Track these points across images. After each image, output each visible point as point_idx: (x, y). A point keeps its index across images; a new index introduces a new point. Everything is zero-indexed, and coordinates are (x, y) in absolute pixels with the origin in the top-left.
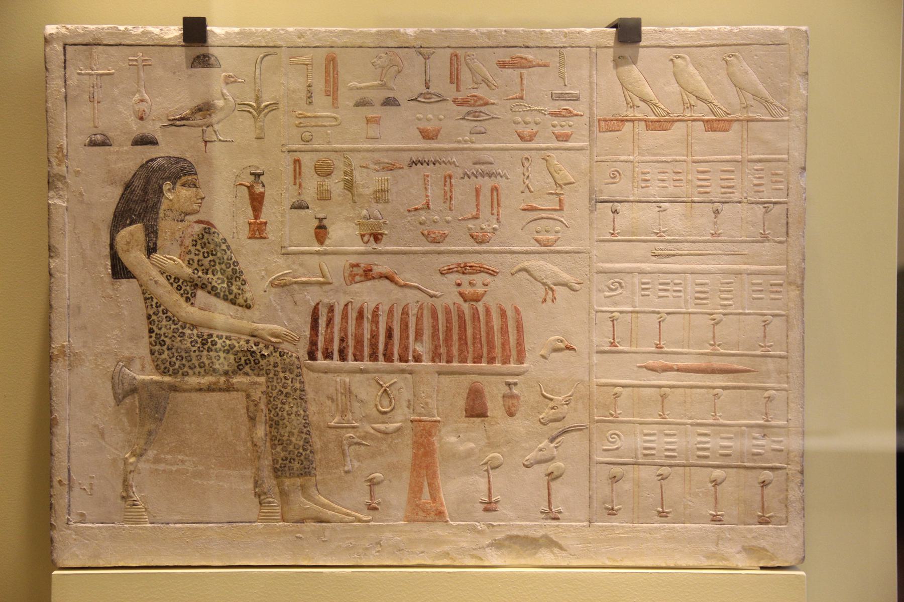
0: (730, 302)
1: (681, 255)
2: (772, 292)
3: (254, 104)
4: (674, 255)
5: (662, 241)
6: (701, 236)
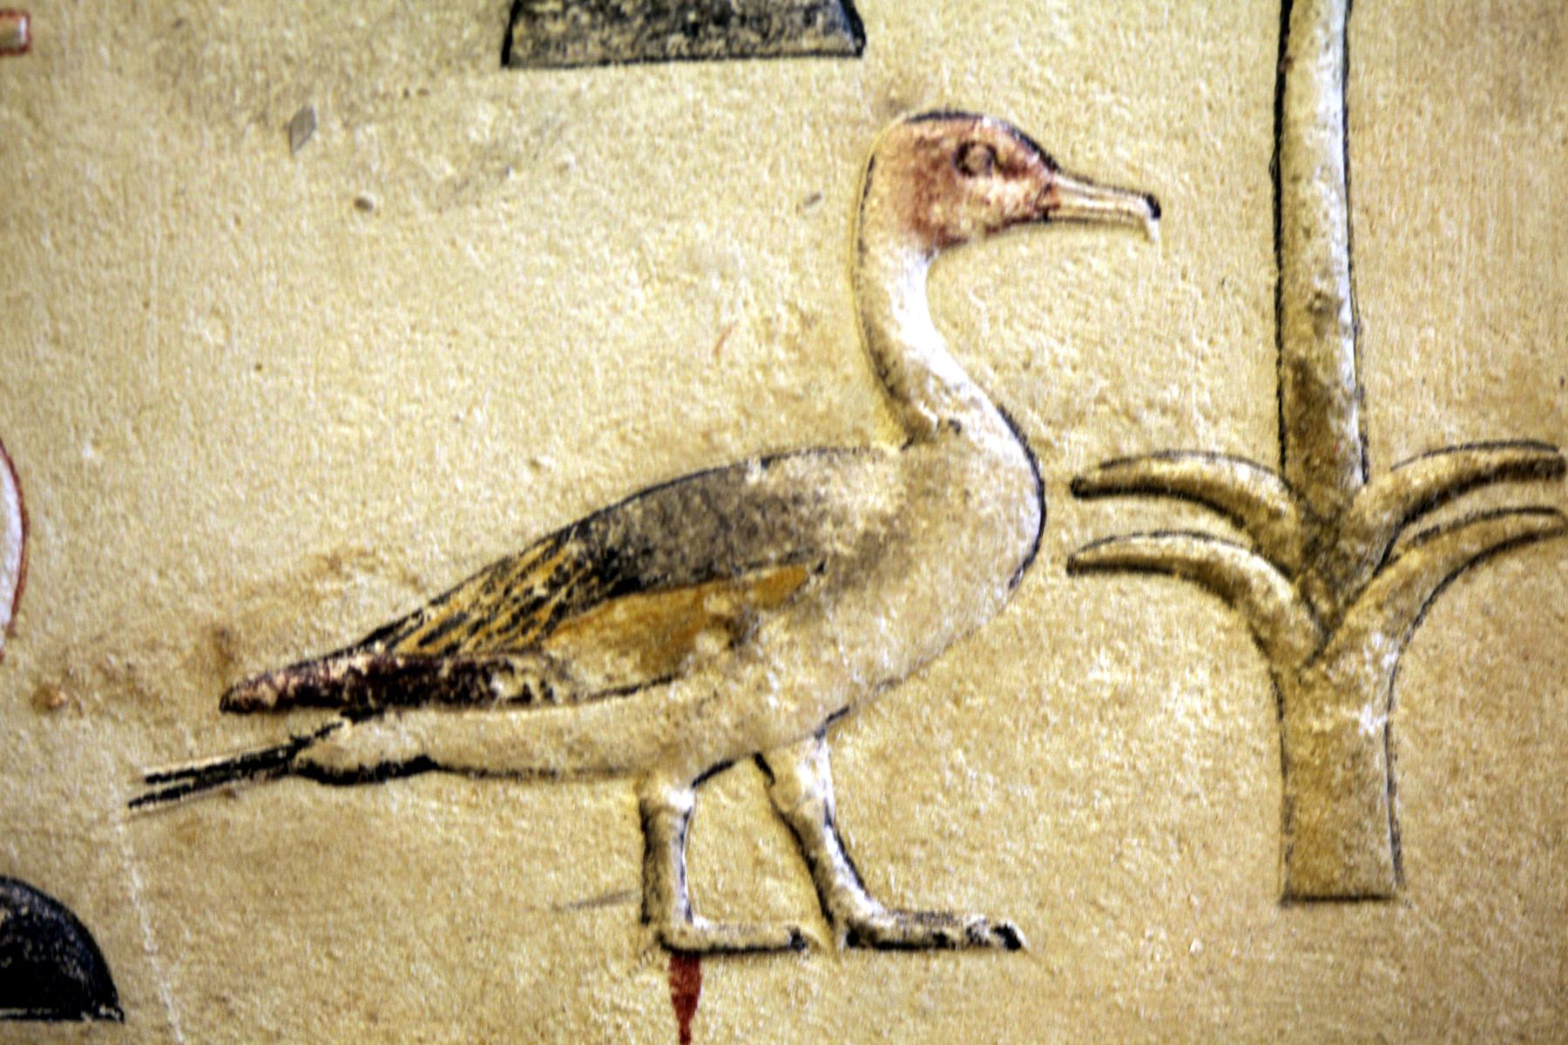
3: (1269, 489)
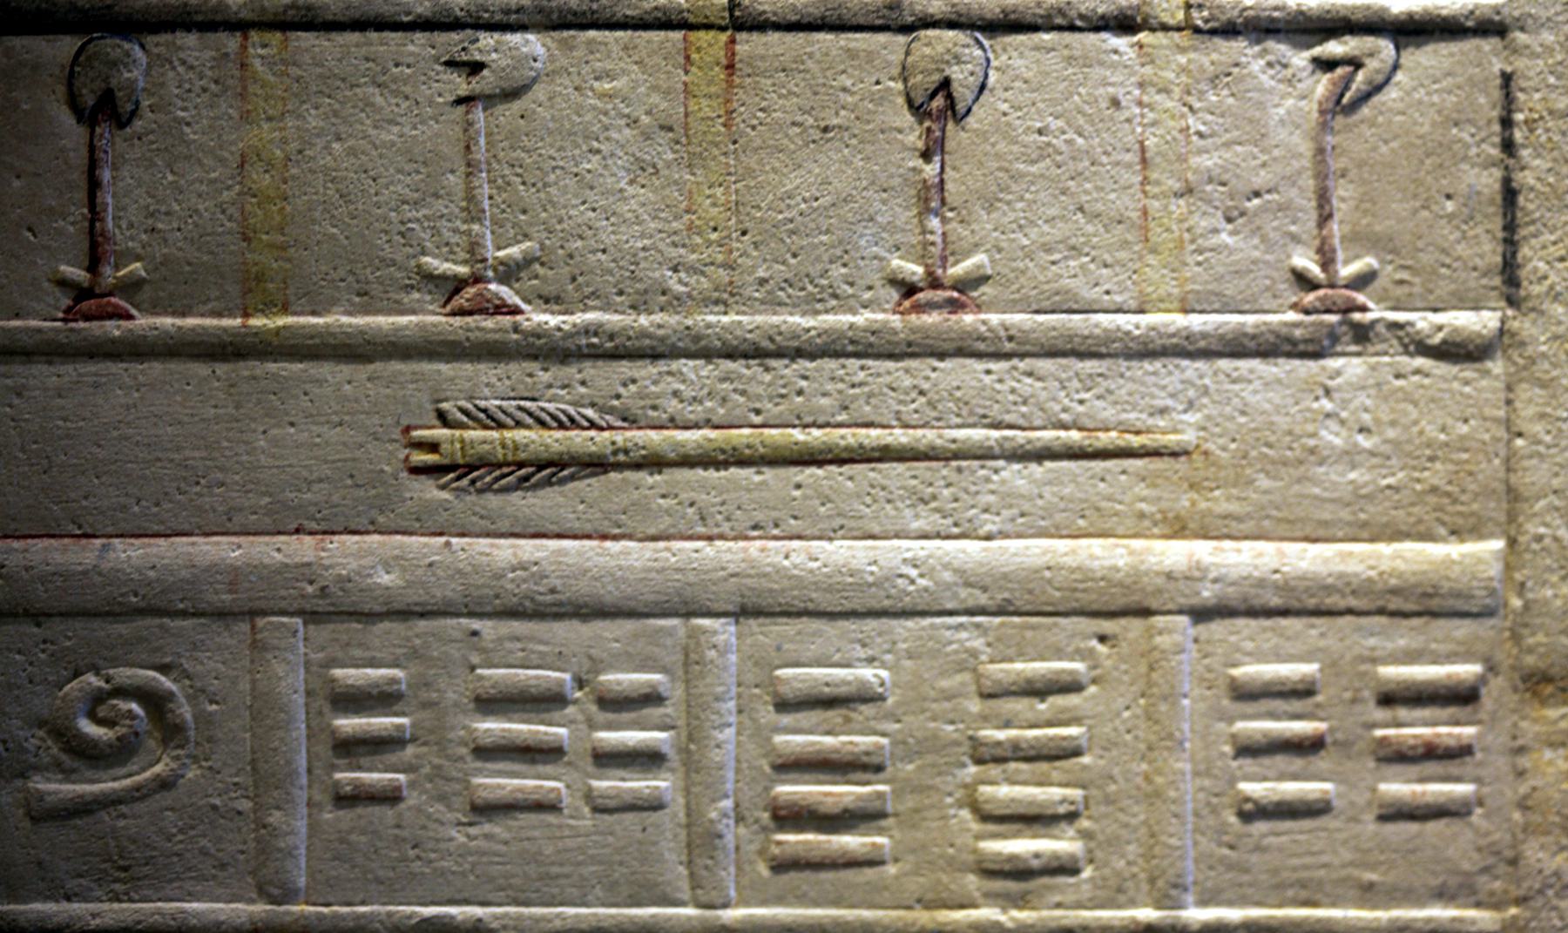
0: (1062, 844)
1: (655, 462)
2: (1398, 757)
4: (597, 465)
5: (493, 352)
6: (811, 305)
